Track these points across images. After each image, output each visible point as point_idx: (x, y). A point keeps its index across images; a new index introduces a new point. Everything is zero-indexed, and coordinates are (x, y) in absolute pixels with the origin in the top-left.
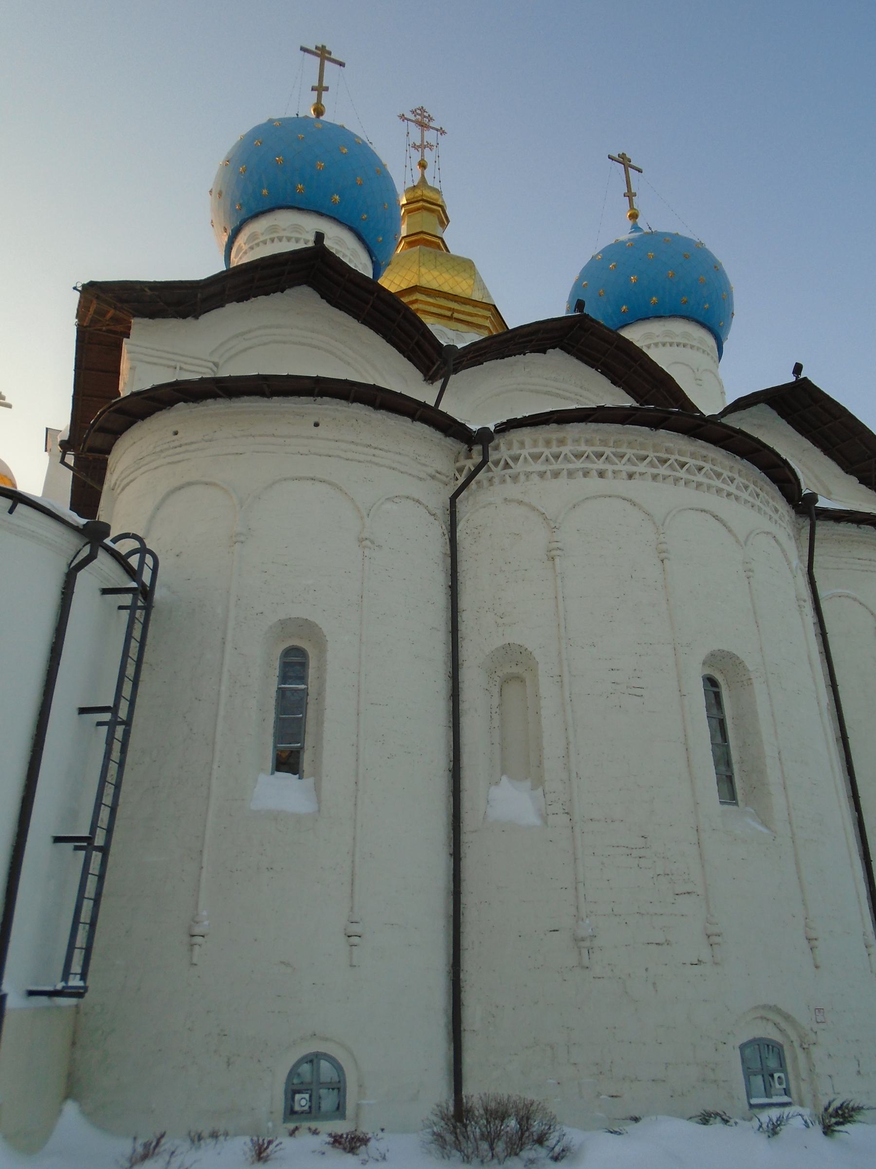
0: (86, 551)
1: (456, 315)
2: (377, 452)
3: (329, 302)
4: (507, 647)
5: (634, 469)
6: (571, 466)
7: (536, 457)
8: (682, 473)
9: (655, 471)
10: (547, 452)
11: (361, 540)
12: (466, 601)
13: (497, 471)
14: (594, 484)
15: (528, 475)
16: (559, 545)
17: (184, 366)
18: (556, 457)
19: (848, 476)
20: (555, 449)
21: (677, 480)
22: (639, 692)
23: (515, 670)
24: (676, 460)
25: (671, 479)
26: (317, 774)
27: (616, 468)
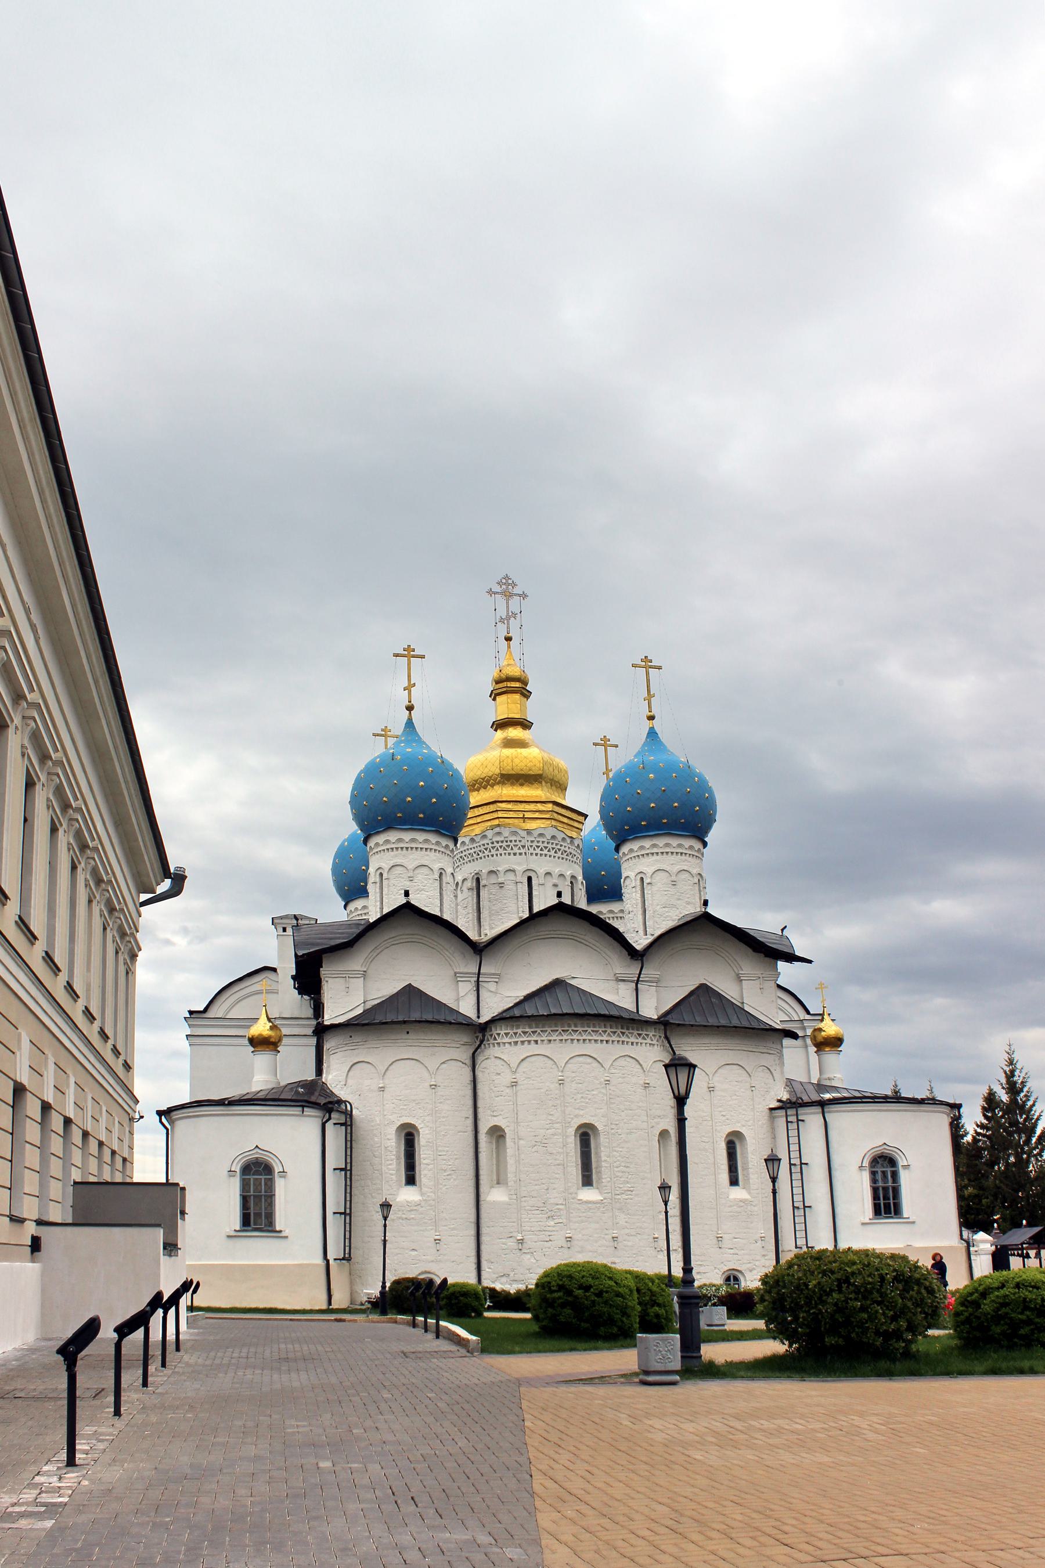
0: (327, 1115)
1: (527, 815)
2: (435, 1041)
3: (418, 915)
4: (495, 1126)
5: (550, 1038)
6: (522, 1039)
7: (507, 1034)
8: (575, 1036)
9: (561, 1038)
10: (511, 1032)
11: (431, 1086)
12: (480, 1104)
13: (492, 1041)
14: (533, 1049)
15: (504, 1043)
16: (515, 1080)
17: (350, 976)
18: (515, 1034)
19: (755, 954)
20: (515, 1031)
21: (572, 1040)
22: (546, 1145)
23: (502, 1134)
24: (572, 1030)
25: (569, 1041)
26: (420, 1186)
27: (542, 1039)
